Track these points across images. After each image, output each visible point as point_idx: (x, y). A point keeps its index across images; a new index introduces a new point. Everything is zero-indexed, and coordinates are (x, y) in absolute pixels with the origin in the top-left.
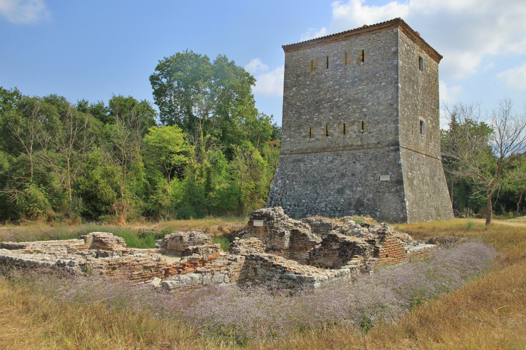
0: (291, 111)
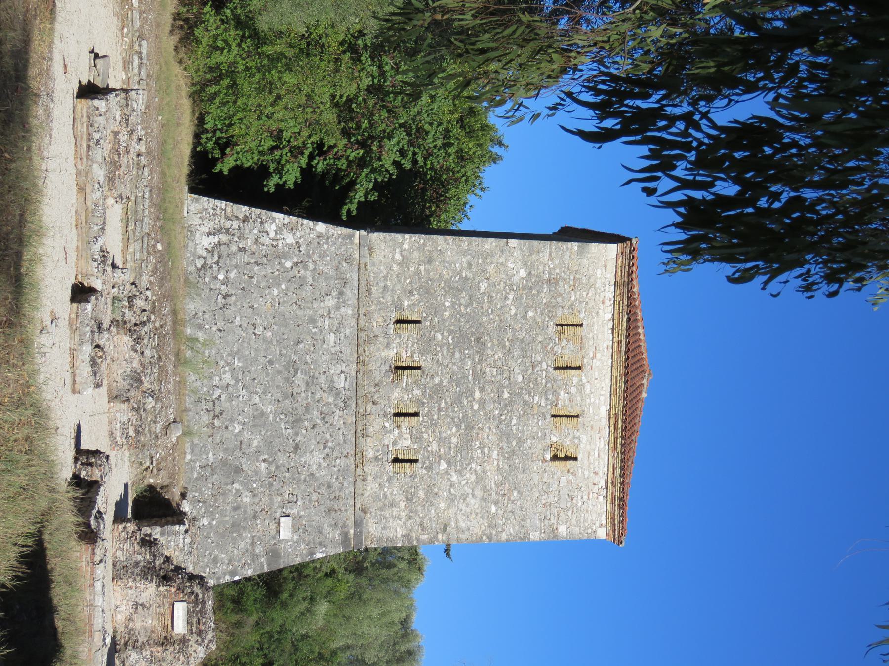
0: (470, 264)
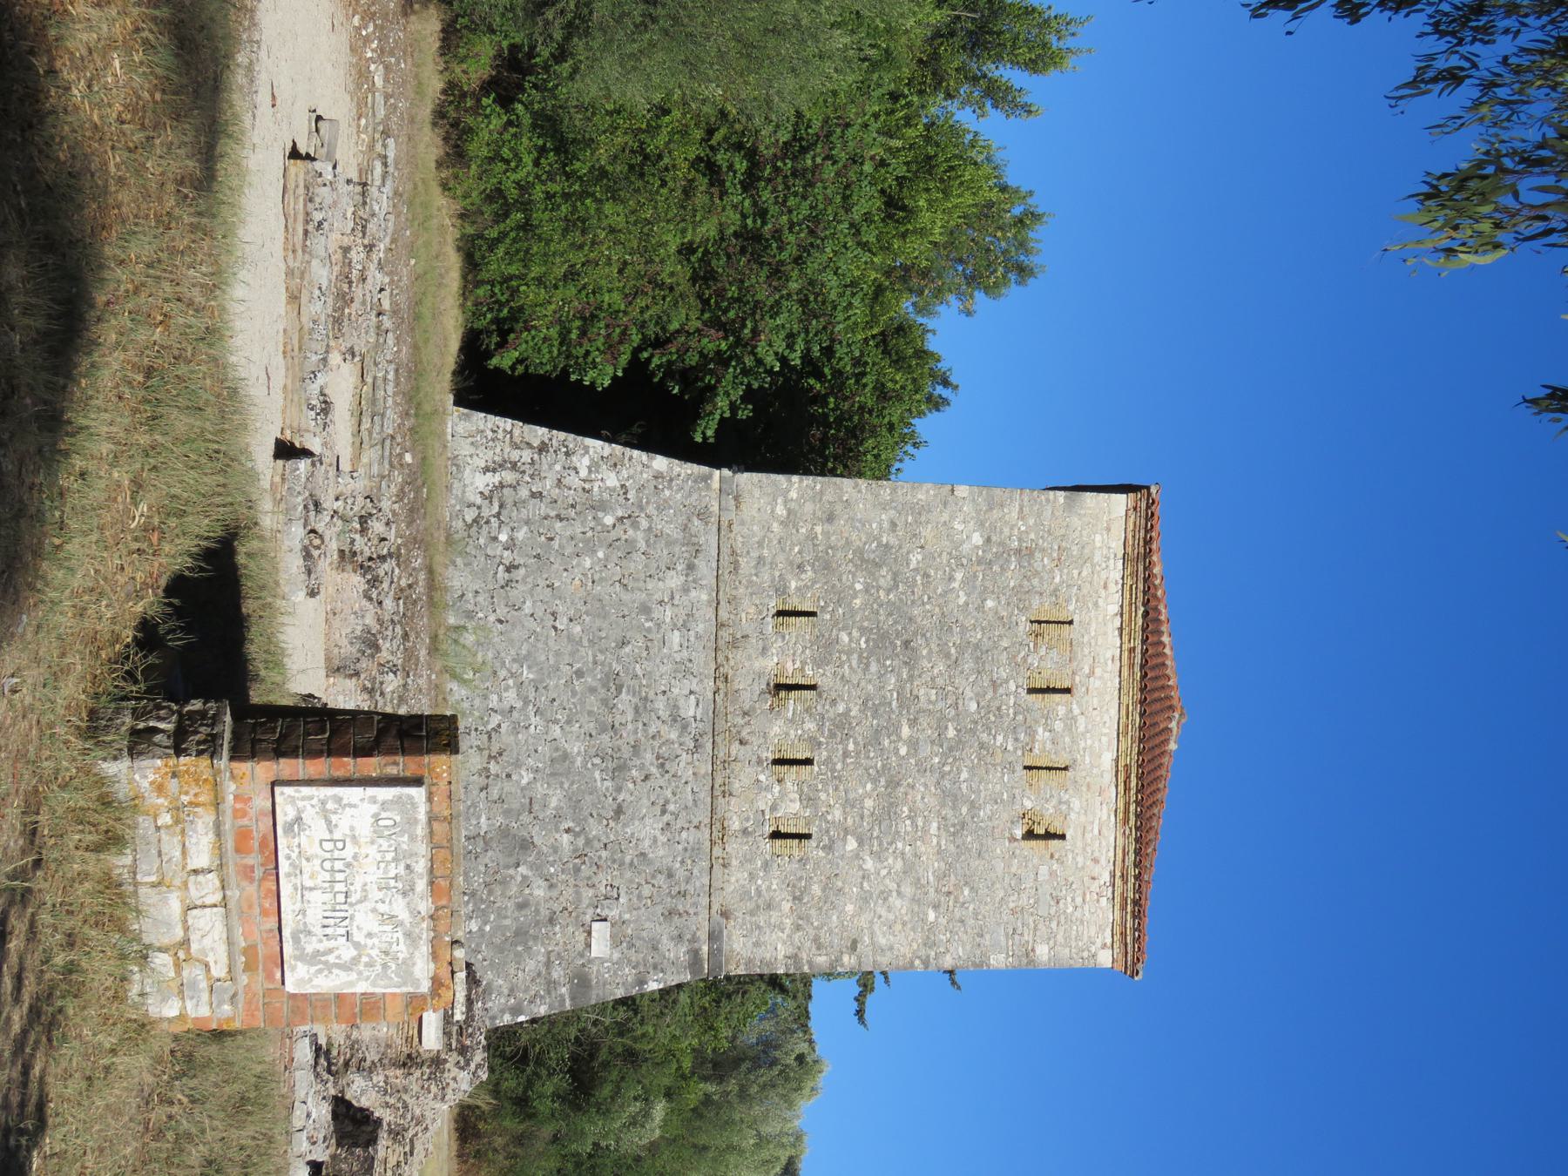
0: (893, 525)
